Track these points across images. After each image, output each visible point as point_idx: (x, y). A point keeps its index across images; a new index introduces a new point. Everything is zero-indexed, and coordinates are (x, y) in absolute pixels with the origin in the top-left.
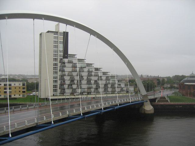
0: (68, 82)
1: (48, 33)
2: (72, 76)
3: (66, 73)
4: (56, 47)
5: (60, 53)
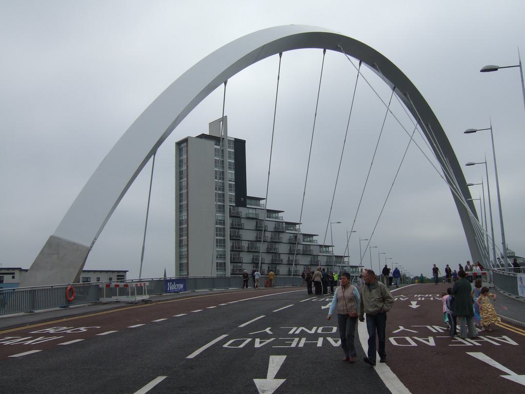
1: (201, 139)
2: (257, 254)
3: (245, 245)
4: (222, 175)
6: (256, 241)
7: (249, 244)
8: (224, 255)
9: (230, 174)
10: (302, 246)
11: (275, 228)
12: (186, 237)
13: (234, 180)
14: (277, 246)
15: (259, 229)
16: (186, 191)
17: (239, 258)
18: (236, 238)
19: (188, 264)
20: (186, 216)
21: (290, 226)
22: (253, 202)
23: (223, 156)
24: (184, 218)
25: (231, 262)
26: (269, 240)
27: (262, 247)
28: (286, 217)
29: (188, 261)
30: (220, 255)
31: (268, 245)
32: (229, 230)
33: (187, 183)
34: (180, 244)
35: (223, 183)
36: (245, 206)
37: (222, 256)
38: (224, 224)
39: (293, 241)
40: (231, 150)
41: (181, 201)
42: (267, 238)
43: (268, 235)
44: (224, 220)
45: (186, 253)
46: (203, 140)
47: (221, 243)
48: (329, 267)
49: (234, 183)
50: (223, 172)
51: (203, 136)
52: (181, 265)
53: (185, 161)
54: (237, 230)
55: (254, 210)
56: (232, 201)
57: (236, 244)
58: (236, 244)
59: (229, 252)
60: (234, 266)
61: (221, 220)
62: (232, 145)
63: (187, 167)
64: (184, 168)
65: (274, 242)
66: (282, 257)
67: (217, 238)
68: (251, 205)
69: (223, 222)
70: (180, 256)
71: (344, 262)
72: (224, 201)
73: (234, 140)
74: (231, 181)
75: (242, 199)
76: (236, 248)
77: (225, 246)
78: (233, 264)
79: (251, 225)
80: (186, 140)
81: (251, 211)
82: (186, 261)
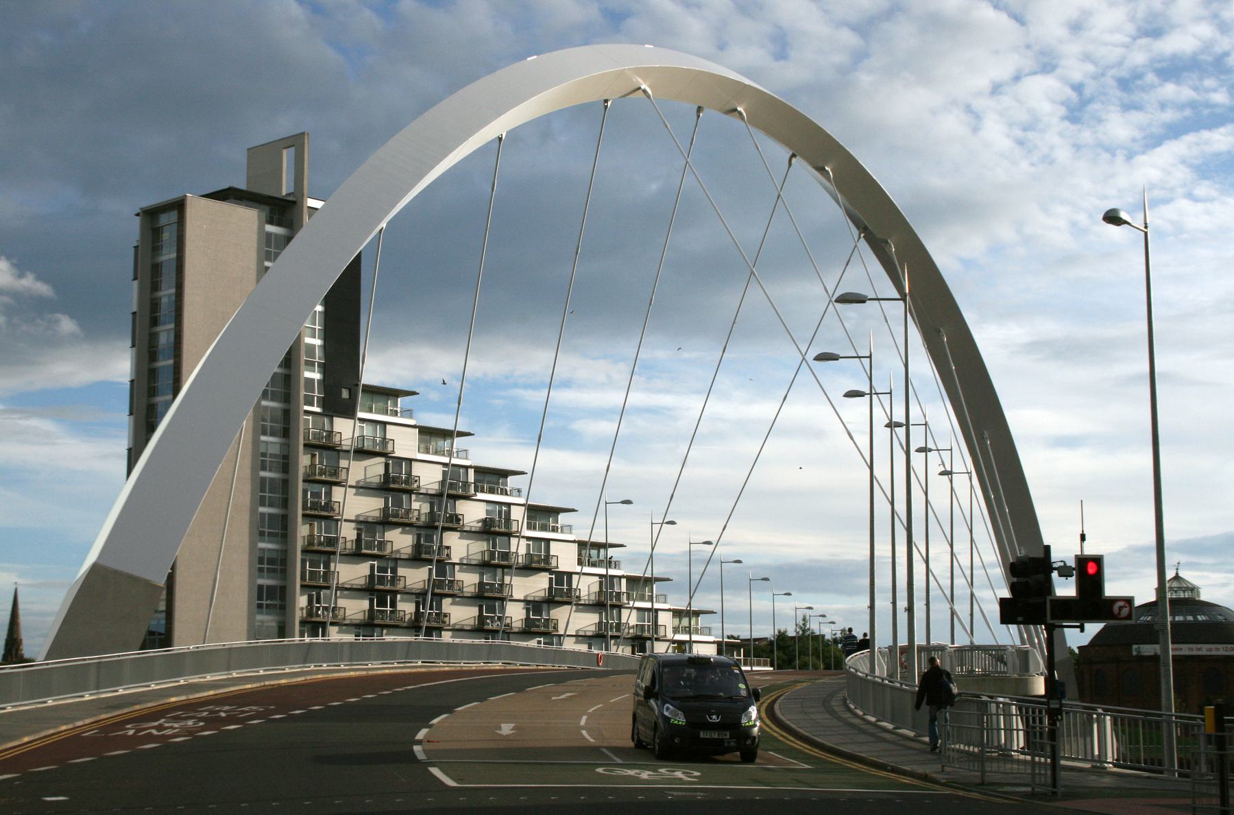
3: (348, 532)
16: (171, 362)
27: (401, 541)
65: (429, 529)
75: (345, 394)
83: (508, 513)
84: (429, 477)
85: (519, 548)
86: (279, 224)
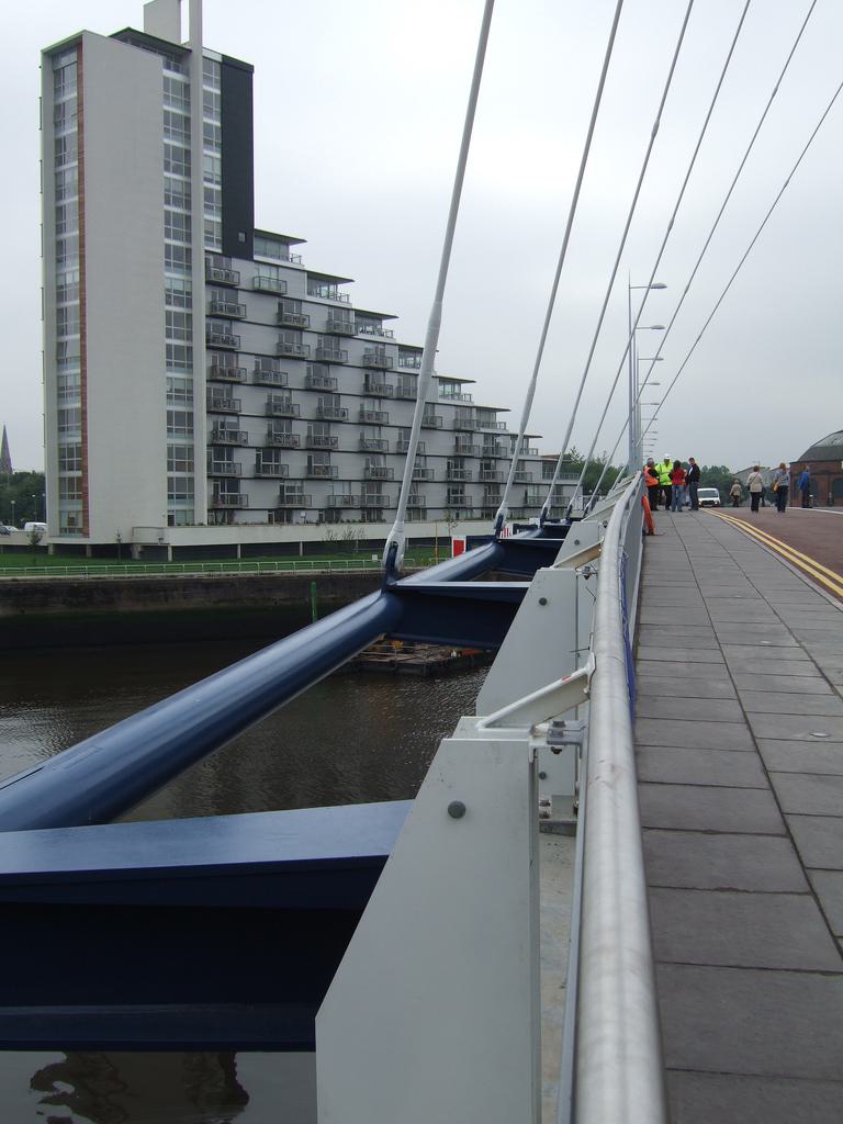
0: (255, 432)
2: (278, 393)
3: (247, 365)
4: (182, 161)
5: (206, 120)
6: (277, 358)
7: (257, 363)
8: (190, 392)
9: (209, 160)
10: (396, 376)
11: (329, 322)
12: (78, 336)
13: (219, 179)
14: (334, 372)
15: (287, 324)
16: (76, 198)
17: (230, 402)
18: (222, 347)
19: (84, 412)
20: (78, 274)
21: (367, 321)
22: (272, 247)
23: (187, 105)
24: (71, 276)
25: (208, 412)
26: (313, 357)
27: (295, 374)
28: (358, 297)
29: (84, 403)
30: (177, 391)
31: (308, 369)
32: (204, 320)
33: (81, 174)
34: (57, 355)
35: (188, 185)
36: (250, 258)
37: (183, 394)
38: (189, 304)
39: (374, 367)
40: (209, 121)
41: (60, 229)
42: (306, 350)
43: (310, 341)
44: (189, 294)
45: (77, 279)
46: (128, 49)
47: (180, 357)
48: (461, 435)
49: (218, 188)
50: (188, 153)
51: (127, 36)
52: (62, 415)
53: (71, 110)
54: (226, 324)
55: (274, 270)
56: (212, 240)
57: (221, 363)
58: (221, 363)
59: (205, 385)
60: (215, 423)
61: (181, 292)
62: (216, 76)
63: (81, 126)
64: (70, 130)
66: (345, 403)
67: (169, 341)
68: (265, 255)
69: (186, 299)
70: (60, 388)
71: (493, 424)
72: (188, 238)
73: (219, 59)
74: (210, 181)
75: (242, 236)
76: (222, 372)
77: (190, 366)
78: (215, 417)
79: (265, 310)
80: (75, 44)
81: (265, 272)
82: (78, 405)
83: (383, 350)
84: (317, 320)
85: (392, 380)
86: (177, 70)
